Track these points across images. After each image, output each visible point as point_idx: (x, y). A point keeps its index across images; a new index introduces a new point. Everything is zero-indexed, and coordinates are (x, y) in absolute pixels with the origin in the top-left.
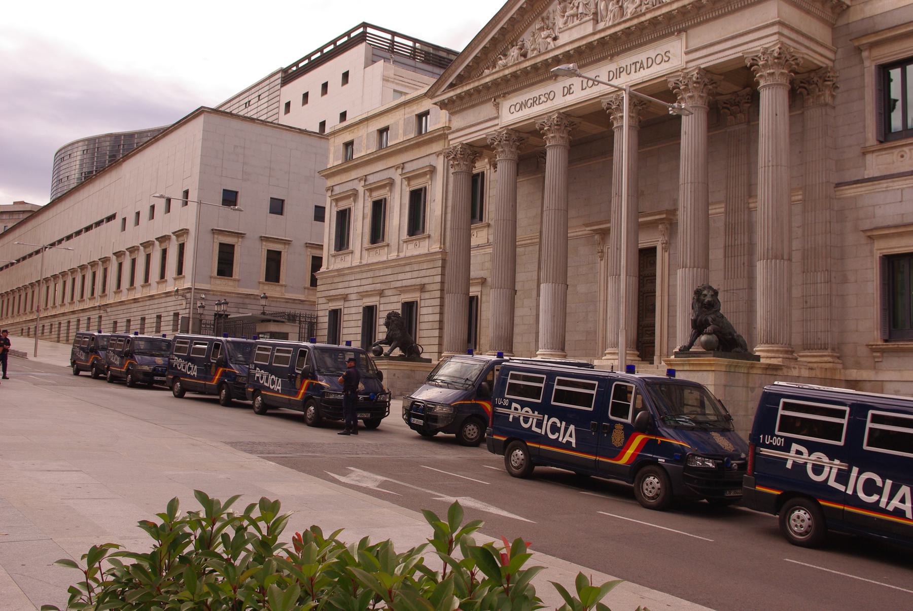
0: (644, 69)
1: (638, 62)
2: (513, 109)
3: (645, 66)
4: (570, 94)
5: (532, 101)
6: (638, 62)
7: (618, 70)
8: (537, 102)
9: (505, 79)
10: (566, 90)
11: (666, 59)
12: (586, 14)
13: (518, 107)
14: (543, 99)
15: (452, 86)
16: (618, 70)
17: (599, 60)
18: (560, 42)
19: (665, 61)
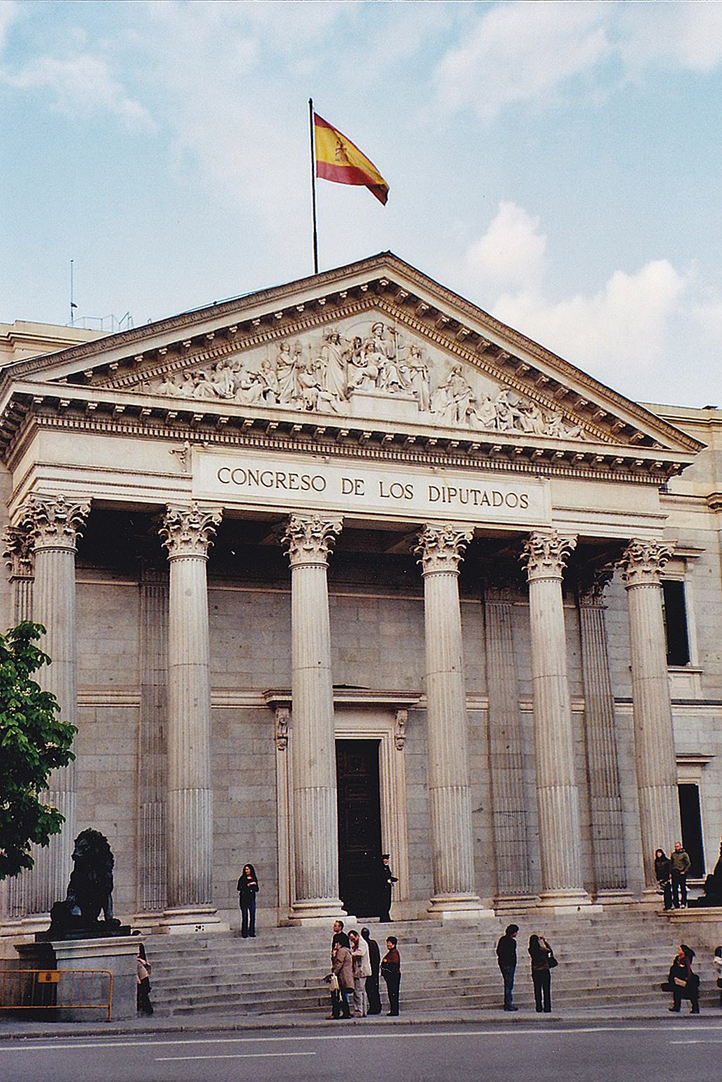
0: (489, 505)
1: (479, 492)
2: (226, 476)
3: (492, 504)
4: (356, 494)
5: (274, 478)
6: (479, 492)
7: (446, 490)
8: (287, 483)
9: (236, 422)
10: (348, 487)
11: (525, 505)
12: (400, 387)
13: (239, 477)
14: (298, 482)
15: (78, 379)
16: (446, 490)
17: (411, 463)
18: (342, 408)
19: (522, 507)
